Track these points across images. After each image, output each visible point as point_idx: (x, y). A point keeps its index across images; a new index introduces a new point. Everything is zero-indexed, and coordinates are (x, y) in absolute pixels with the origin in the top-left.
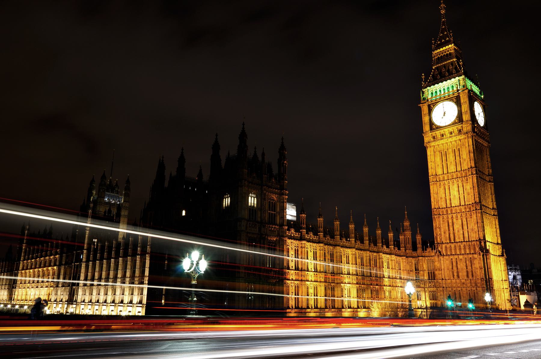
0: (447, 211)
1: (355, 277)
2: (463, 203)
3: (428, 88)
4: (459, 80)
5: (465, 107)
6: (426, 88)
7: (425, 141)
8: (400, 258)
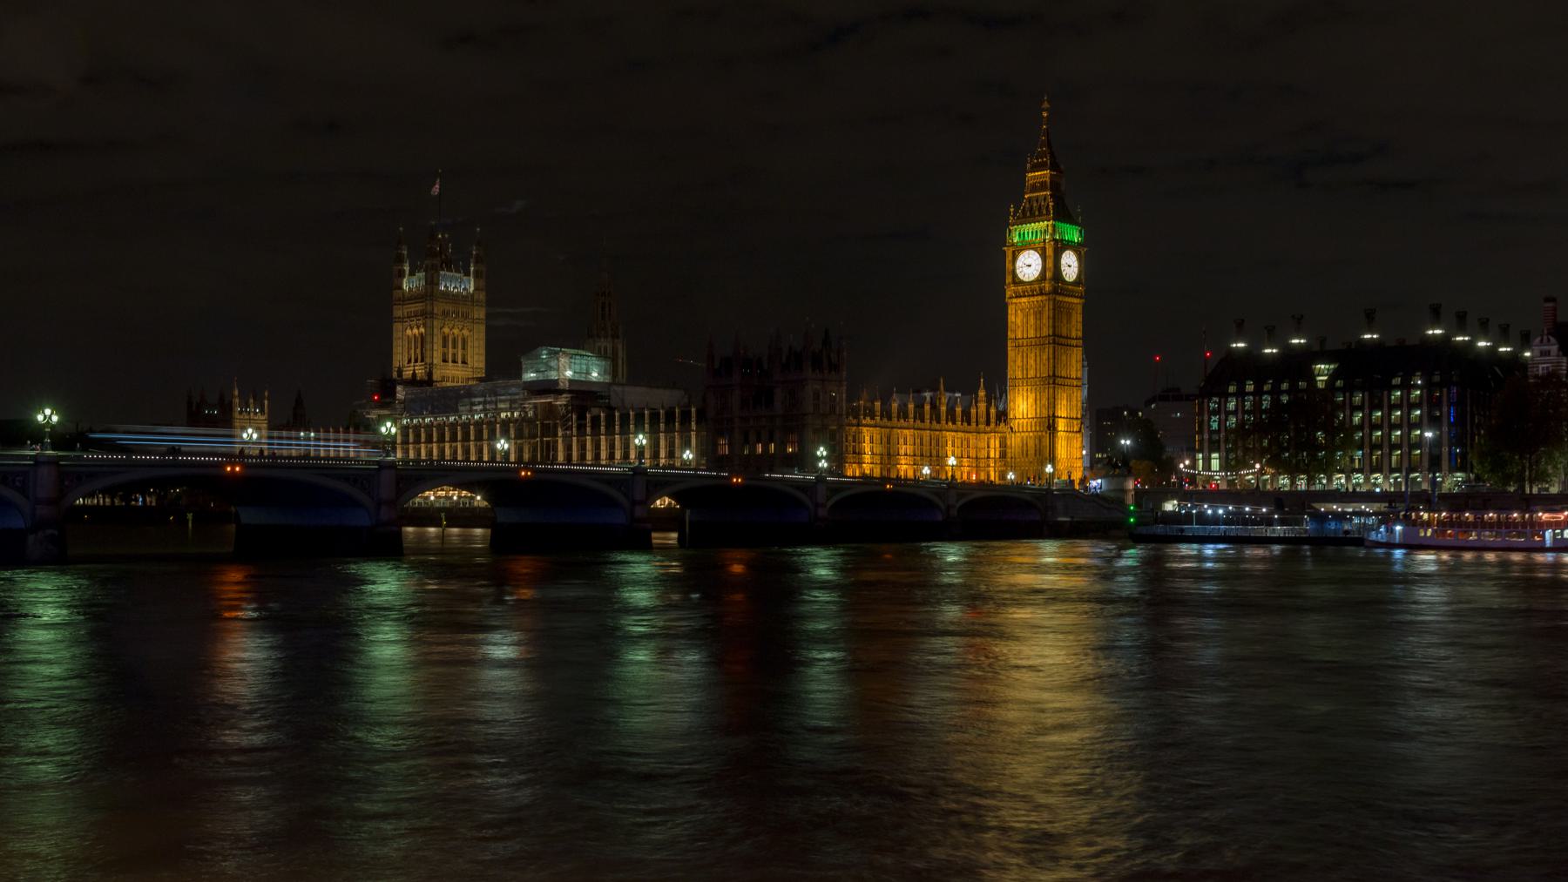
0: (1023, 382)
1: (912, 459)
2: (1038, 375)
3: (1016, 227)
4: (1048, 225)
5: (1050, 264)
6: (1013, 225)
7: (1007, 296)
8: (970, 435)
